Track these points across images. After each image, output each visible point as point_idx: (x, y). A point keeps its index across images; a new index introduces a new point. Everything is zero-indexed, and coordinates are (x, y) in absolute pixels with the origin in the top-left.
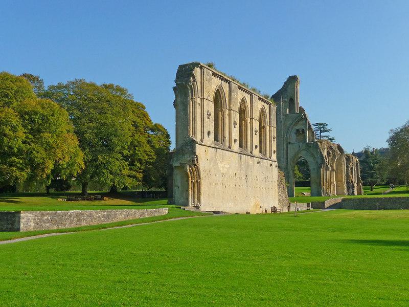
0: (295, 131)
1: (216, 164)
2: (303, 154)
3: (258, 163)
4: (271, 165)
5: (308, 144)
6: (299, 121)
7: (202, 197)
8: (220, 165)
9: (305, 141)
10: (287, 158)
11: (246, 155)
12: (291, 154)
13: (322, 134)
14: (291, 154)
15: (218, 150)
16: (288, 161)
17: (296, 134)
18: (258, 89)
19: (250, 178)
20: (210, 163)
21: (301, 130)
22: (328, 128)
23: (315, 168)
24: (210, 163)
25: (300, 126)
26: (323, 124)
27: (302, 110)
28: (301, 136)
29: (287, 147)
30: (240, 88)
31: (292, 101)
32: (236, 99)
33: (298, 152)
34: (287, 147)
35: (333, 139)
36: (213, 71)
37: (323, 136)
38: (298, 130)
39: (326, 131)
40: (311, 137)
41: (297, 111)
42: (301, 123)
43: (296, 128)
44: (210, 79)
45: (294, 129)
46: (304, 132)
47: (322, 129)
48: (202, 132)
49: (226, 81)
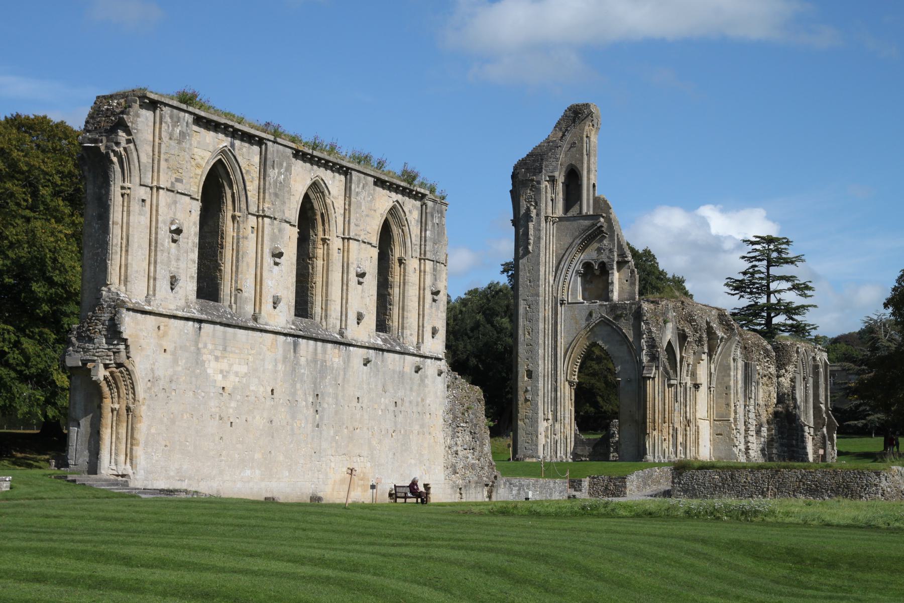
1: (198, 361)
3: (367, 362)
4: (418, 369)
5: (614, 308)
7: (139, 451)
8: (212, 367)
9: (608, 298)
11: (316, 340)
13: (774, 271)
15: (205, 326)
17: (583, 276)
18: (376, 157)
19: (328, 404)
20: (175, 361)
22: (791, 253)
24: (175, 361)
26: (777, 239)
27: (602, 206)
30: (299, 155)
32: (283, 187)
35: (807, 288)
36: (197, 111)
39: (789, 261)
41: (587, 208)
44: (183, 135)
46: (605, 270)
47: (774, 255)
48: (152, 278)
49: (249, 138)
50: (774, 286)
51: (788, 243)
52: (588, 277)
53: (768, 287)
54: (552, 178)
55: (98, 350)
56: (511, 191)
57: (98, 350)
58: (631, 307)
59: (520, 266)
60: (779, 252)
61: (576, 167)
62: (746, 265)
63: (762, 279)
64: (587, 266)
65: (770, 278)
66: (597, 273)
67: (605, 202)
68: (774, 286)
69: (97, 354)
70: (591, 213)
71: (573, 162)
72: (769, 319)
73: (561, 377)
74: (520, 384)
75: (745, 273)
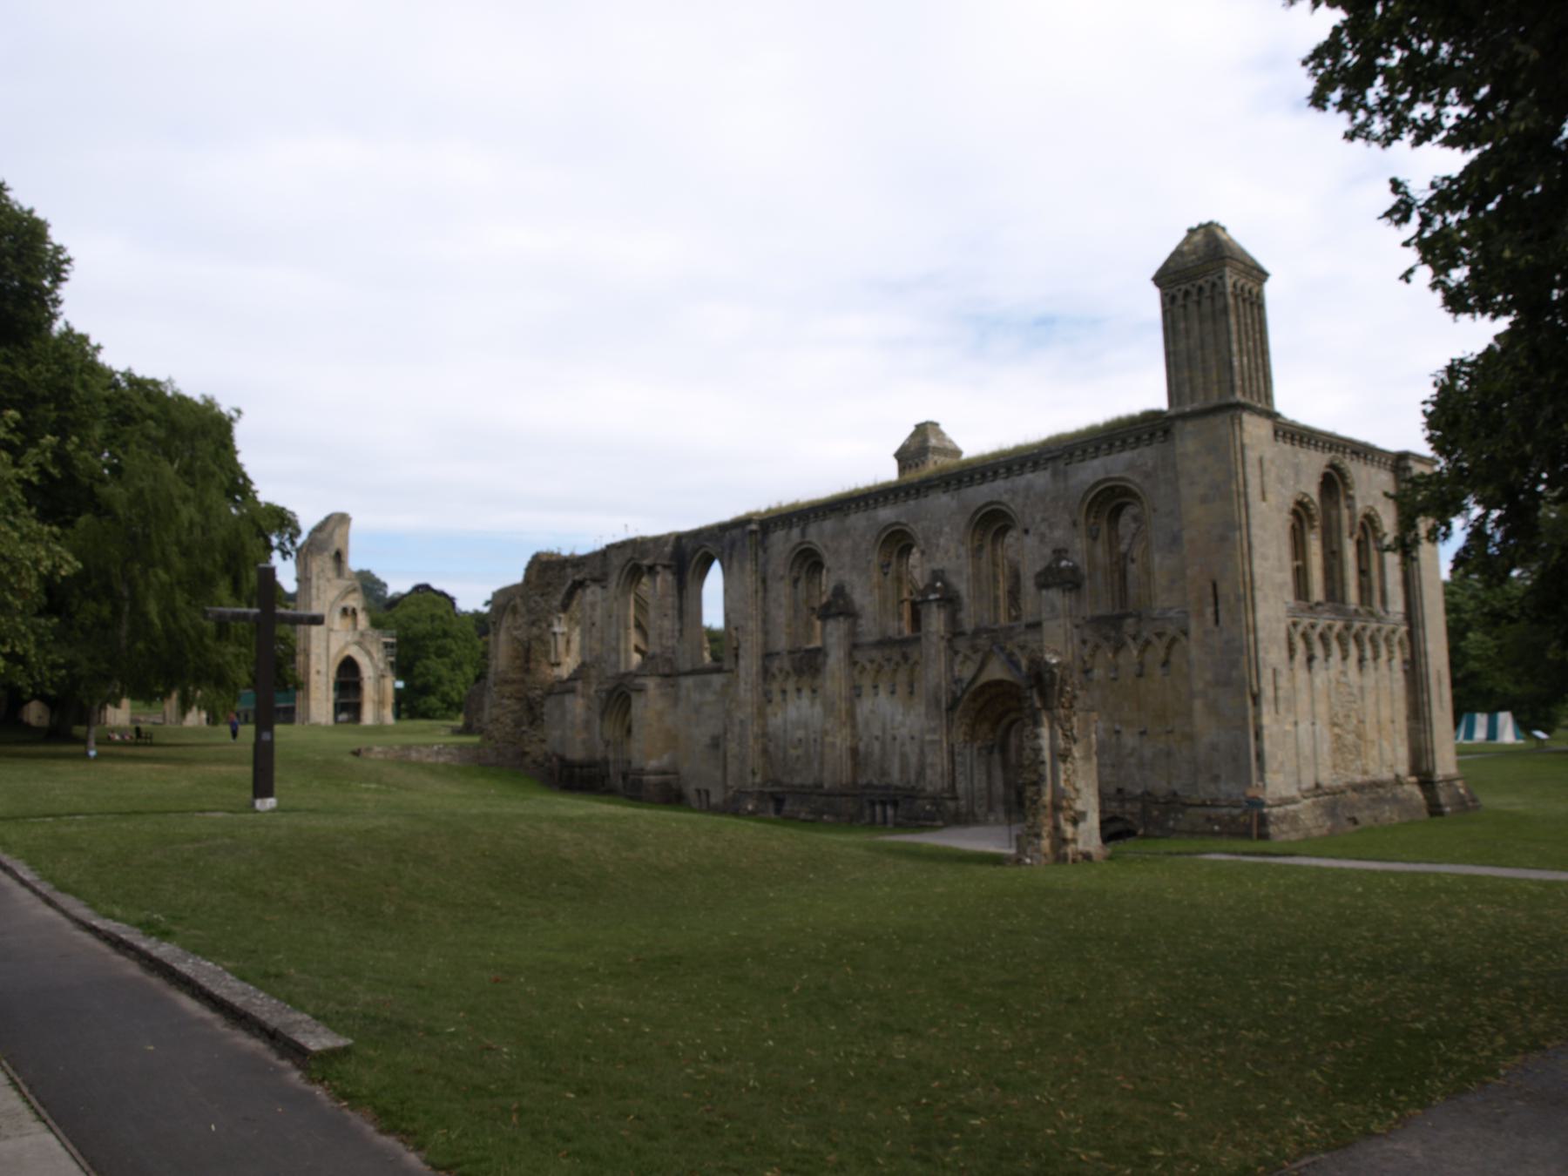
2: (354, 651)
6: (349, 592)
12: (334, 649)
28: (348, 621)
33: (347, 645)
38: (345, 611)
64: (345, 611)
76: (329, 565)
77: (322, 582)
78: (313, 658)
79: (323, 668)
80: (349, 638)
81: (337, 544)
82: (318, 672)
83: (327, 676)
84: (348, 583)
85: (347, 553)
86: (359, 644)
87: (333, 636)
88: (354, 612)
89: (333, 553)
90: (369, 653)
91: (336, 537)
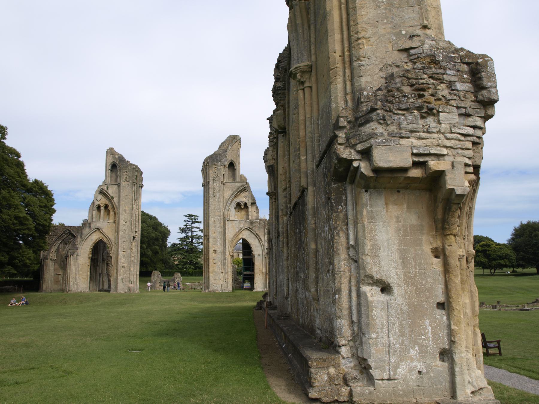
0: (235, 205)
2: (246, 235)
6: (241, 192)
10: (225, 240)
12: (230, 234)
13: (194, 225)
14: (230, 234)
16: (225, 243)
21: (242, 205)
23: (261, 253)
25: (243, 199)
27: (244, 180)
28: (243, 213)
29: (225, 224)
31: (232, 166)
33: (240, 231)
34: (225, 224)
37: (195, 227)
38: (238, 205)
40: (255, 214)
42: (243, 194)
43: (237, 200)
45: (234, 201)
47: (194, 220)
50: (193, 230)
51: (198, 217)
52: (237, 210)
53: (192, 230)
54: (224, 165)
55: (449, 135)
56: (203, 170)
57: (449, 135)
58: (260, 223)
59: (210, 202)
60: (195, 219)
61: (234, 161)
62: (185, 223)
63: (190, 227)
64: (238, 205)
65: (192, 228)
66: (243, 207)
67: (245, 177)
68: (193, 230)
69: (448, 143)
70: (240, 181)
71: (232, 159)
72: (192, 240)
73: (228, 254)
74: (210, 256)
75: (185, 226)
76: (224, 171)
77: (217, 184)
78: (211, 240)
79: (219, 248)
80: (242, 226)
81: (229, 157)
82: (215, 251)
83: (225, 253)
84: (239, 184)
85: (239, 163)
86: (249, 229)
87: (229, 225)
88: (245, 204)
89: (227, 164)
90: (257, 236)
91: (229, 153)
